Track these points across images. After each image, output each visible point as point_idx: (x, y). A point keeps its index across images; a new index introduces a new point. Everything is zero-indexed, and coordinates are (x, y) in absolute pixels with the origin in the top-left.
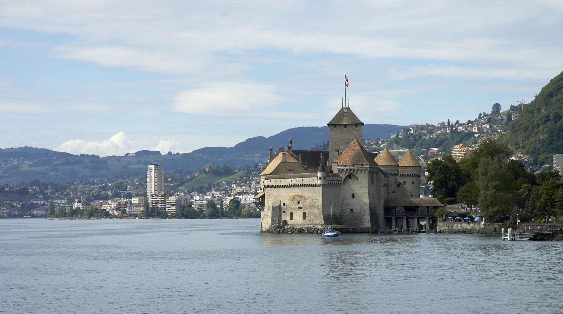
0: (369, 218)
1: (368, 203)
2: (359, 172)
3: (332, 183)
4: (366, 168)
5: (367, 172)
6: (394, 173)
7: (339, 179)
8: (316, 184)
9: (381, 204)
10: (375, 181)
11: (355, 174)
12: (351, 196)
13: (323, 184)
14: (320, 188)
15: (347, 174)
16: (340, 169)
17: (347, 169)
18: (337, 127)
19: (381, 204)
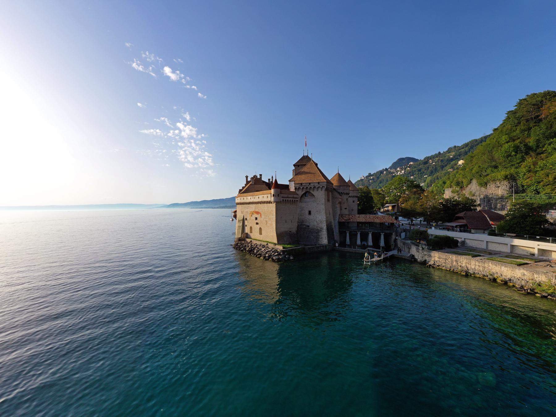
0: (326, 235)
1: (325, 220)
2: (316, 190)
3: (288, 200)
4: (323, 186)
5: (324, 189)
6: (346, 193)
7: (295, 196)
8: (270, 201)
9: (336, 220)
10: (330, 199)
11: (312, 192)
12: (307, 212)
13: (278, 201)
14: (274, 205)
15: (304, 192)
16: (297, 187)
17: (303, 187)
18: (300, 166)
19: (336, 220)
